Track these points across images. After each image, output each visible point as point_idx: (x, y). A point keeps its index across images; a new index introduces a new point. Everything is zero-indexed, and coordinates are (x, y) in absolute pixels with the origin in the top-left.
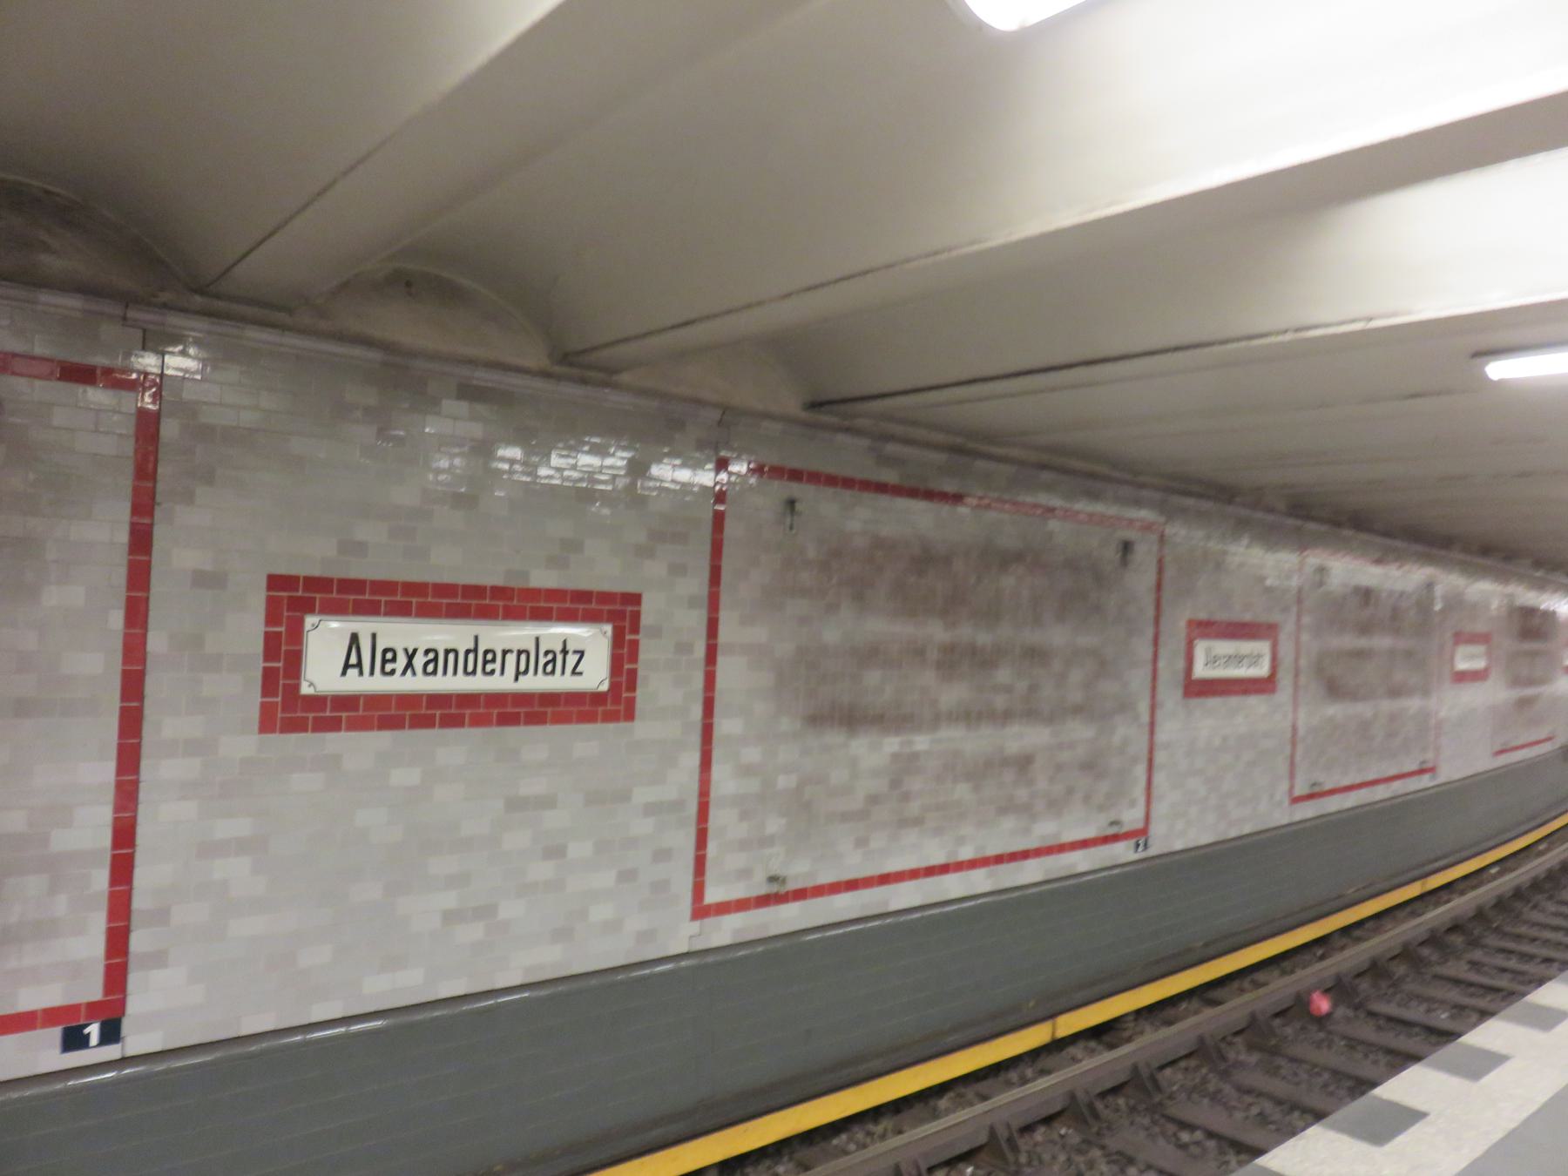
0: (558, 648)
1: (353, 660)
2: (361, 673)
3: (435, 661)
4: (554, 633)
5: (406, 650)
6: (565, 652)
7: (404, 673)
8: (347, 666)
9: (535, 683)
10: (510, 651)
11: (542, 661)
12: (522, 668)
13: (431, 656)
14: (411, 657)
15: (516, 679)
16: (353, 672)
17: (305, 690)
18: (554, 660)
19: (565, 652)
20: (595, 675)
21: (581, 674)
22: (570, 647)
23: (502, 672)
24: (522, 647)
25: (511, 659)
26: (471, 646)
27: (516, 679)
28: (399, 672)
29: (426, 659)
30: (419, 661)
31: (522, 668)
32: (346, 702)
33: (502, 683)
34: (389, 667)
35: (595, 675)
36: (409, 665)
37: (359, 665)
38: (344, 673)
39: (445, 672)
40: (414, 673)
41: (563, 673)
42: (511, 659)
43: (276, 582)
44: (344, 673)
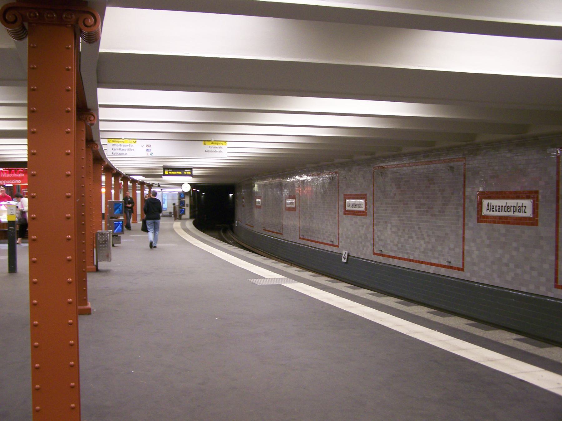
0: (521, 205)
3: (500, 209)
4: (520, 202)
6: (522, 206)
7: (495, 211)
8: (487, 209)
9: (517, 214)
10: (512, 206)
11: (518, 209)
12: (514, 211)
14: (496, 207)
15: (514, 213)
16: (488, 211)
17: (483, 214)
18: (520, 209)
19: (522, 206)
20: (529, 213)
21: (525, 212)
22: (524, 205)
23: (511, 212)
24: (514, 205)
25: (512, 208)
26: (505, 205)
27: (514, 213)
28: (494, 211)
30: (497, 208)
31: (514, 211)
32: (487, 217)
33: (511, 214)
34: (493, 210)
35: (529, 213)
36: (496, 209)
37: (489, 209)
38: (487, 211)
39: (501, 212)
41: (522, 212)
42: (512, 208)
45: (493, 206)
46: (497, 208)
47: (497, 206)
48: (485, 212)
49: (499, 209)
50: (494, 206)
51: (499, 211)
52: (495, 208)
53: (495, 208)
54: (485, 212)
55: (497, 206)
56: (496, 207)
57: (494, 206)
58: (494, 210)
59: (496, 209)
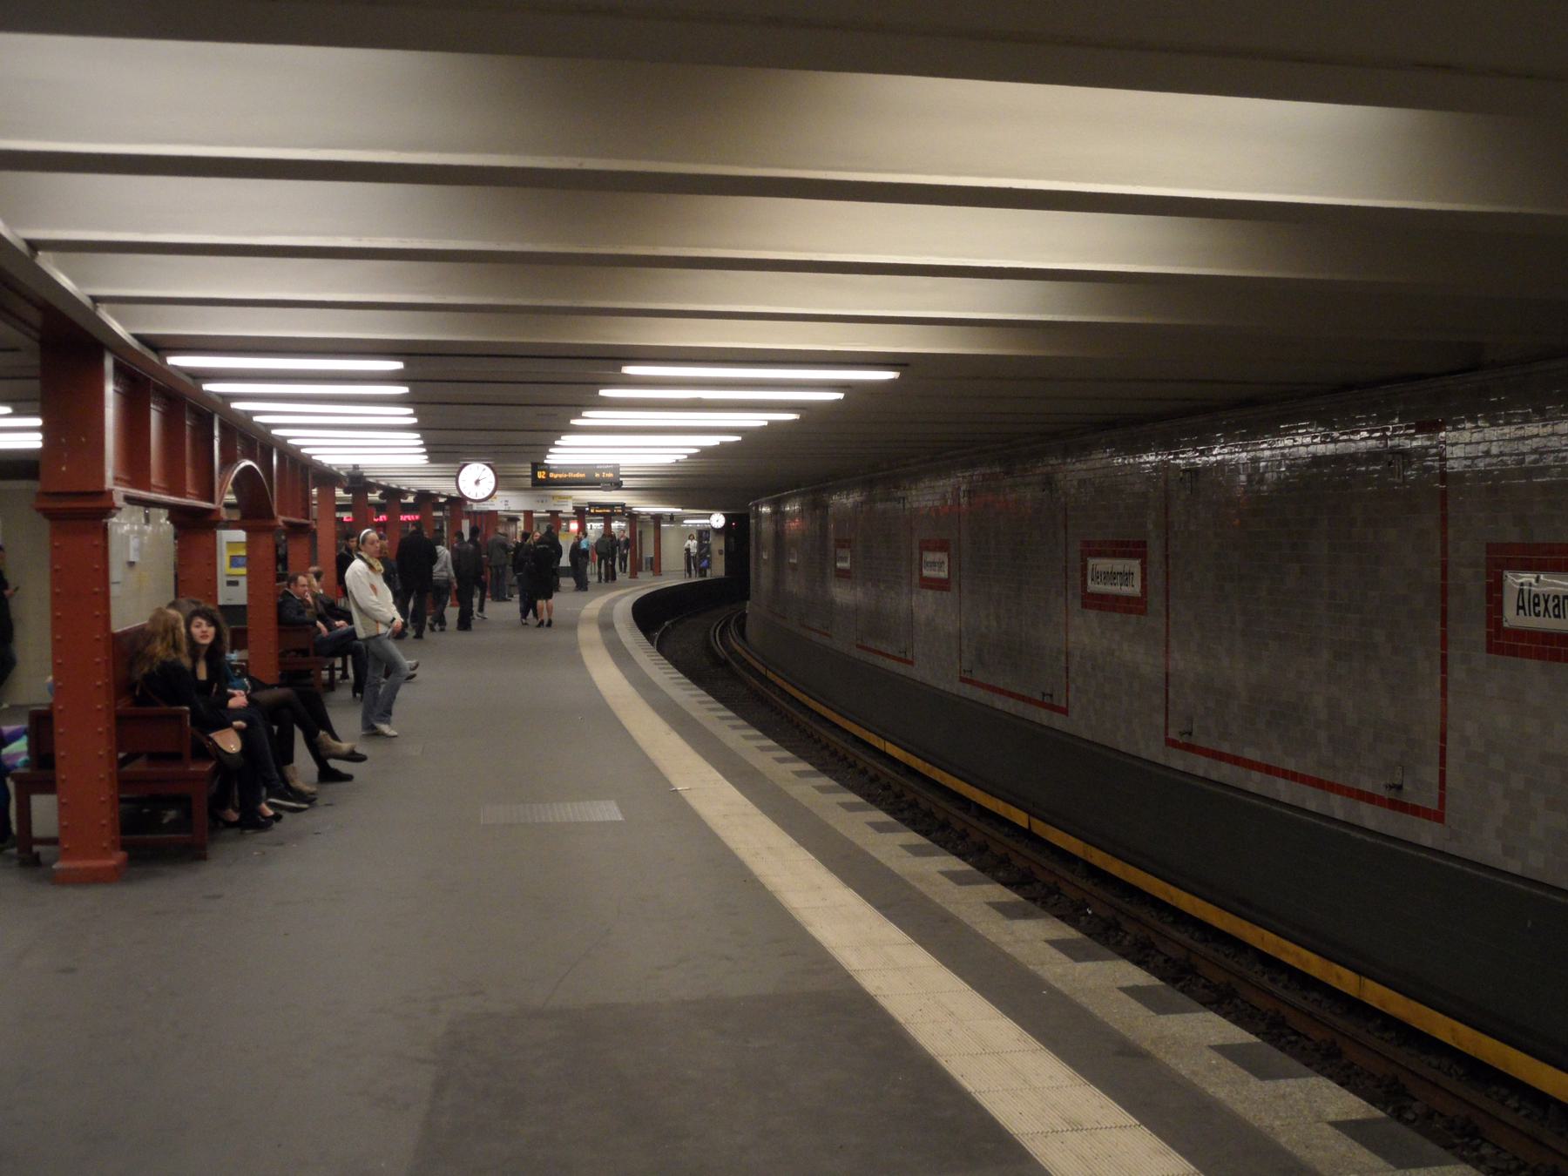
1: (1521, 604)
2: (1525, 614)
5: (1544, 595)
7: (1544, 616)
8: (1519, 608)
13: (1556, 601)
14: (1546, 602)
16: (1521, 611)
29: (1554, 604)
30: (1551, 605)
32: (1520, 634)
34: (1537, 609)
36: (1546, 609)
37: (1523, 608)
38: (1518, 614)
40: (1550, 616)
43: (1491, 548)
44: (1518, 614)
45: (1537, 596)
46: (1551, 605)
47: (1551, 598)
48: (1512, 618)
49: (1557, 606)
50: (1542, 598)
51: (1558, 616)
52: (1542, 603)
53: (1542, 603)
54: (1512, 618)
55: (1551, 598)
56: (1546, 602)
57: (1542, 598)
58: (1541, 608)
59: (1546, 609)
